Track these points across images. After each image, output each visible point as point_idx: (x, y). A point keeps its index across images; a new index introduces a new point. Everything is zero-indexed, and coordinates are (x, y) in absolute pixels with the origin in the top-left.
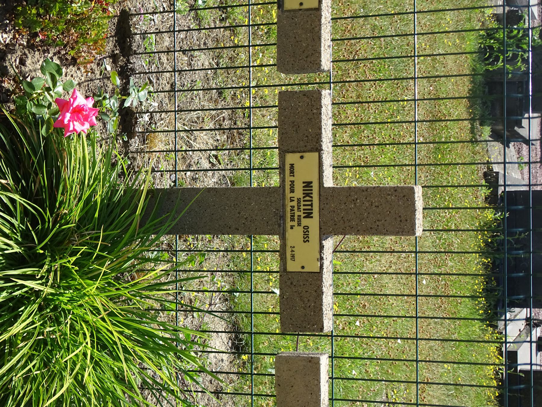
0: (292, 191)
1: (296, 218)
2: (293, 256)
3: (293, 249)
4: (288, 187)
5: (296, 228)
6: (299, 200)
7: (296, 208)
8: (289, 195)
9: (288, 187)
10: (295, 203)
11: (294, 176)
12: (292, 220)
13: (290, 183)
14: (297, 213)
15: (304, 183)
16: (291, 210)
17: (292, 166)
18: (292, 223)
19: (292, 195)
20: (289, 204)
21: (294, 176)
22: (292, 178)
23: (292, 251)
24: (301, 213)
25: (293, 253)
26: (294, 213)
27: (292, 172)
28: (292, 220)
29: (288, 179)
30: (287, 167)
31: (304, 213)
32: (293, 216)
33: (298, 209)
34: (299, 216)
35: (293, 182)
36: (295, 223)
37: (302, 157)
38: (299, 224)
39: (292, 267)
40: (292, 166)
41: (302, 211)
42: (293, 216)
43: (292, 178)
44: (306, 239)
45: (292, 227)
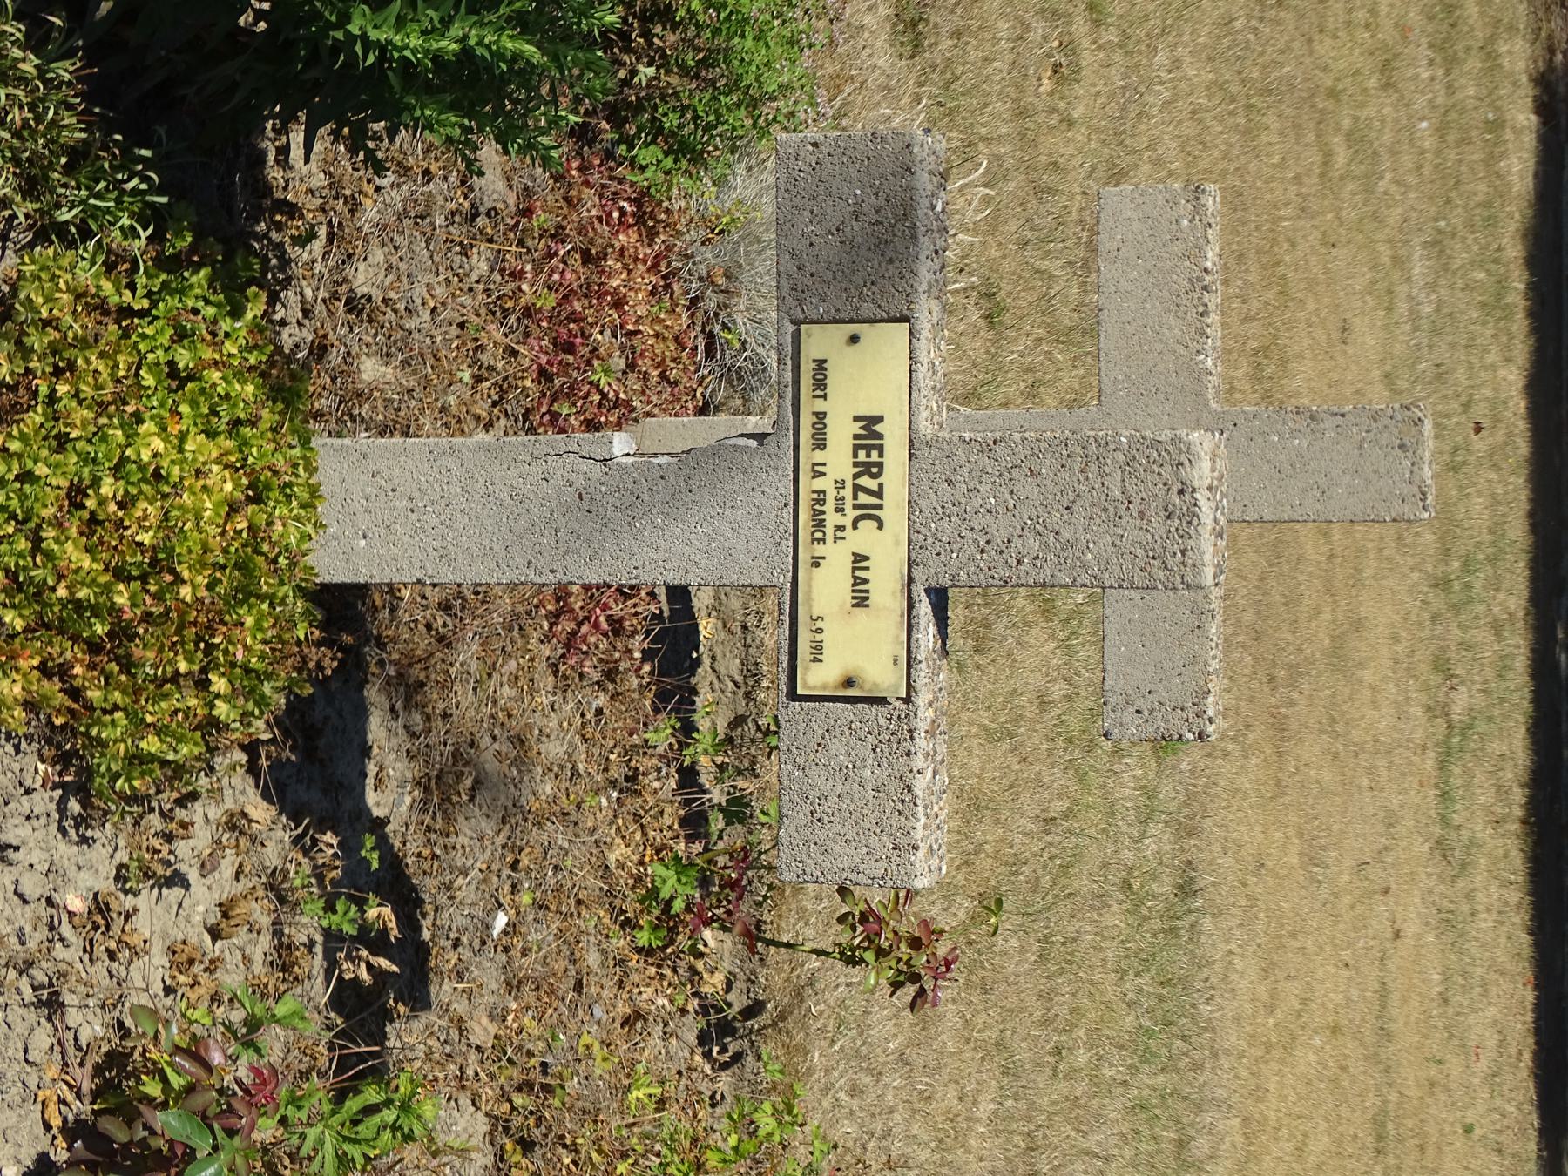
0: (820, 445)
1: (829, 530)
2: (818, 647)
3: (819, 624)
11: (825, 397)
15: (857, 419)
17: (821, 365)
19: (819, 456)
21: (825, 397)
22: (820, 406)
25: (819, 637)
27: (820, 385)
30: (807, 369)
32: (819, 525)
35: (820, 417)
37: (854, 339)
43: (820, 406)
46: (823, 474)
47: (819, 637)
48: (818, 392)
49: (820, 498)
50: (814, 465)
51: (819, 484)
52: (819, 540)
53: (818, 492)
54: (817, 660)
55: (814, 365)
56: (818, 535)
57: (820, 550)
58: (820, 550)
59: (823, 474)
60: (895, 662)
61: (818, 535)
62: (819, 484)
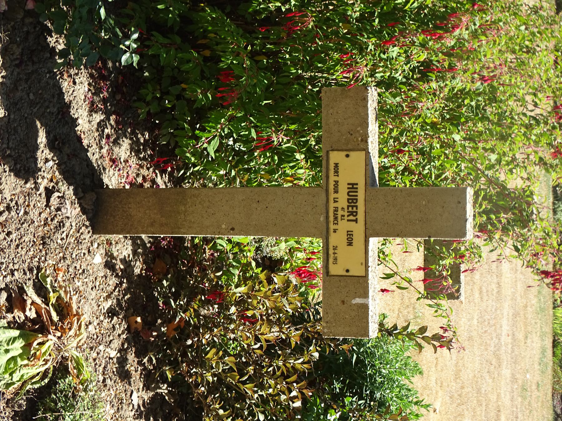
0: (336, 192)
2: (336, 259)
3: (336, 251)
4: (331, 187)
7: (340, 209)
8: (332, 196)
9: (331, 187)
11: (338, 176)
13: (334, 183)
17: (336, 165)
19: (336, 195)
20: (332, 205)
21: (338, 176)
22: (336, 178)
23: (334, 253)
25: (336, 255)
27: (336, 172)
29: (332, 178)
32: (336, 218)
35: (336, 182)
37: (347, 156)
39: (334, 270)
40: (336, 165)
42: (336, 218)
43: (336, 178)
46: (337, 201)
48: (336, 174)
49: (336, 209)
51: (336, 205)
52: (336, 224)
53: (336, 208)
56: (336, 222)
57: (335, 227)
58: (335, 227)
59: (337, 201)
60: (362, 264)
61: (336, 222)
62: (336, 205)
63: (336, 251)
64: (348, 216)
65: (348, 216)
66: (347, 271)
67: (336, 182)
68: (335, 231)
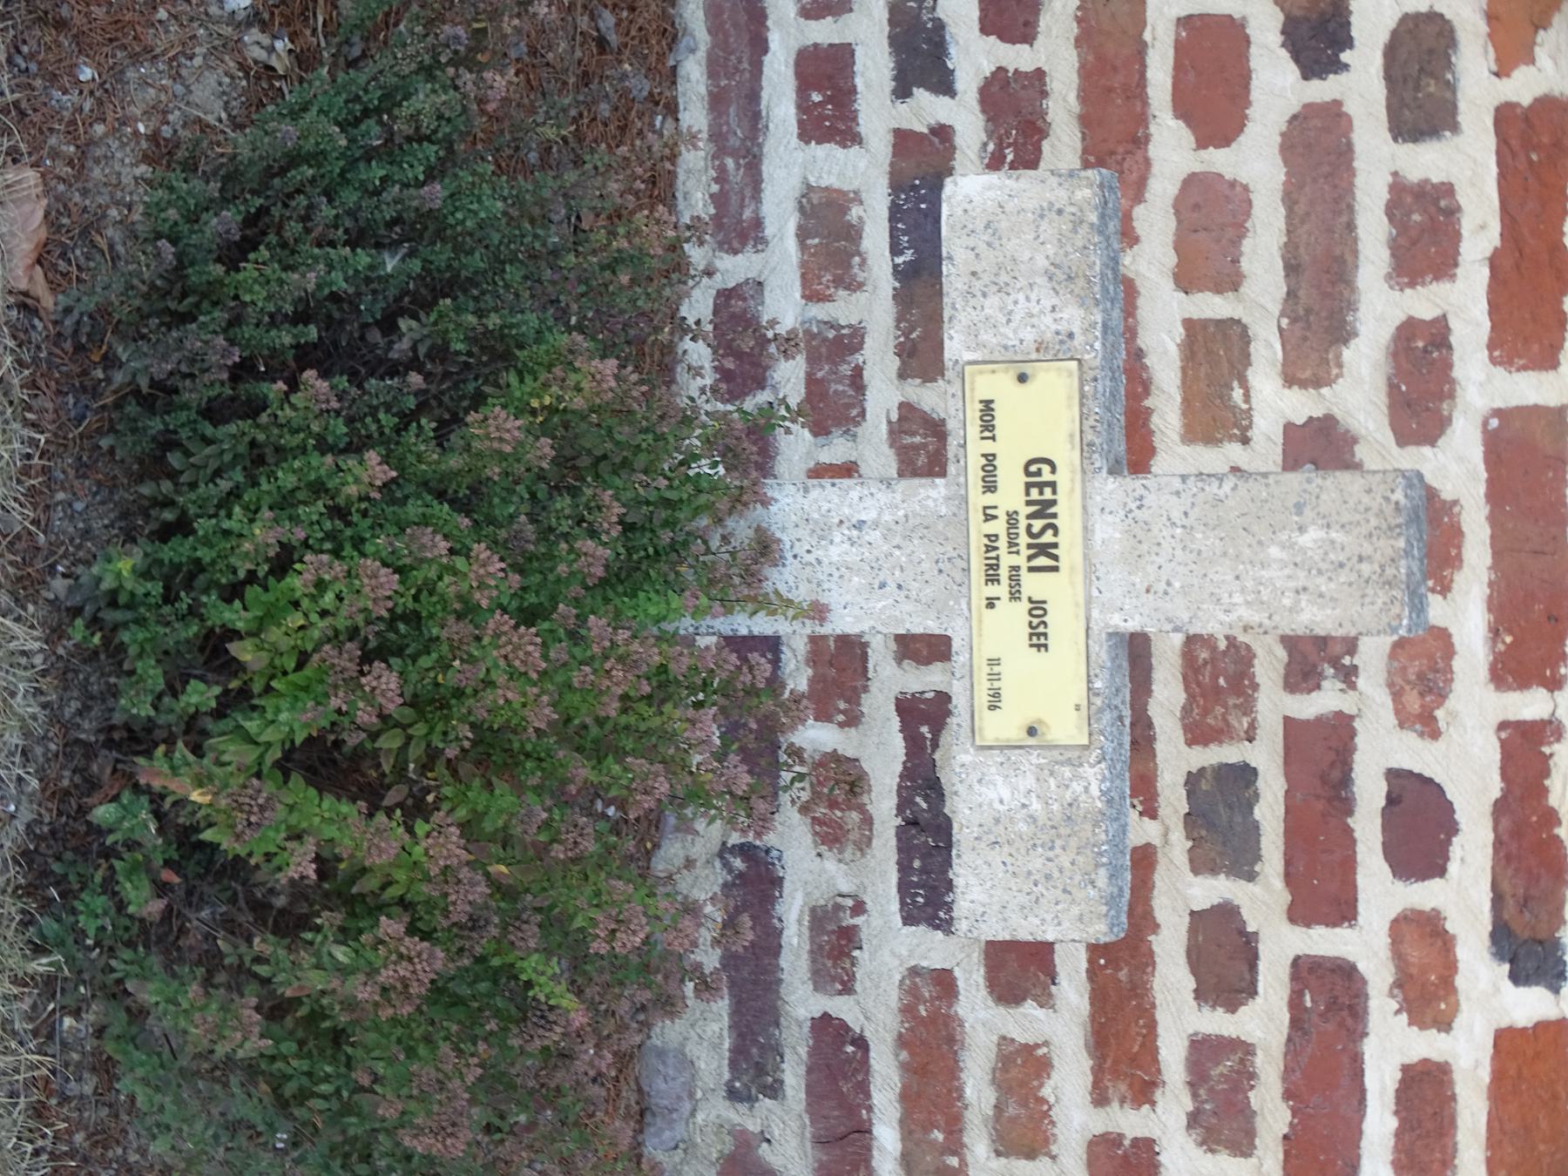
0: (990, 487)
1: (1004, 573)
2: (996, 694)
3: (996, 669)
5: (1004, 605)
6: (1012, 517)
7: (1002, 543)
8: (978, 499)
10: (999, 527)
11: (993, 438)
12: (992, 579)
13: (984, 461)
14: (1007, 560)
16: (989, 549)
17: (988, 405)
18: (992, 590)
19: (989, 499)
20: (978, 530)
21: (993, 438)
22: (988, 447)
24: (1020, 560)
25: (996, 684)
26: (997, 558)
27: (988, 426)
28: (992, 579)
29: (977, 448)
31: (1029, 503)
33: (1011, 544)
34: (1016, 568)
35: (990, 458)
36: (1002, 590)
37: (1022, 378)
38: (1015, 596)
41: (1025, 552)
43: (988, 447)
44: (1038, 638)
45: (991, 604)
46: (995, 517)
47: (996, 684)
48: (987, 434)
50: (985, 508)
51: (991, 527)
53: (987, 536)
54: (992, 708)
55: (981, 406)
59: (995, 517)
60: (1078, 708)
62: (991, 527)
63: (996, 669)
64: (1030, 558)
65: (1030, 558)
66: (1032, 731)
67: (990, 458)
68: (991, 605)
